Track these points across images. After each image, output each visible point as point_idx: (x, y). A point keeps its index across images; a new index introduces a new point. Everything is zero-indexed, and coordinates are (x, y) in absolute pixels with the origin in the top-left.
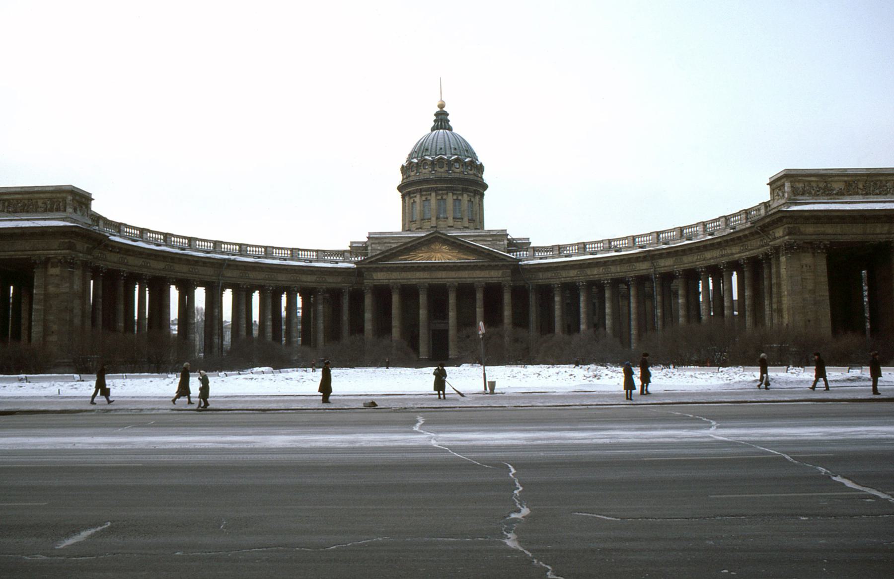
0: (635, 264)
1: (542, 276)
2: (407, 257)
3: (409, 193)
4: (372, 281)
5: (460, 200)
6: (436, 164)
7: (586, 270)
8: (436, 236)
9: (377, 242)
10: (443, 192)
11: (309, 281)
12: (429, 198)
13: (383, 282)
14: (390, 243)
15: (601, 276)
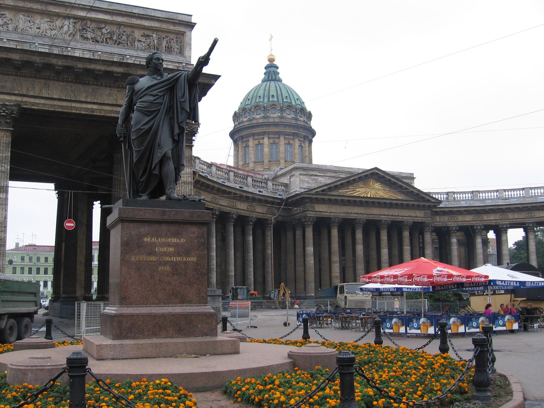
0: (534, 212)
1: (440, 220)
2: (346, 191)
3: (253, 135)
4: (314, 213)
5: (302, 147)
6: (285, 110)
7: (482, 215)
8: (375, 172)
9: (305, 173)
10: (290, 137)
11: (242, 208)
12: (277, 141)
13: (325, 215)
14: (317, 176)
15: (499, 221)
